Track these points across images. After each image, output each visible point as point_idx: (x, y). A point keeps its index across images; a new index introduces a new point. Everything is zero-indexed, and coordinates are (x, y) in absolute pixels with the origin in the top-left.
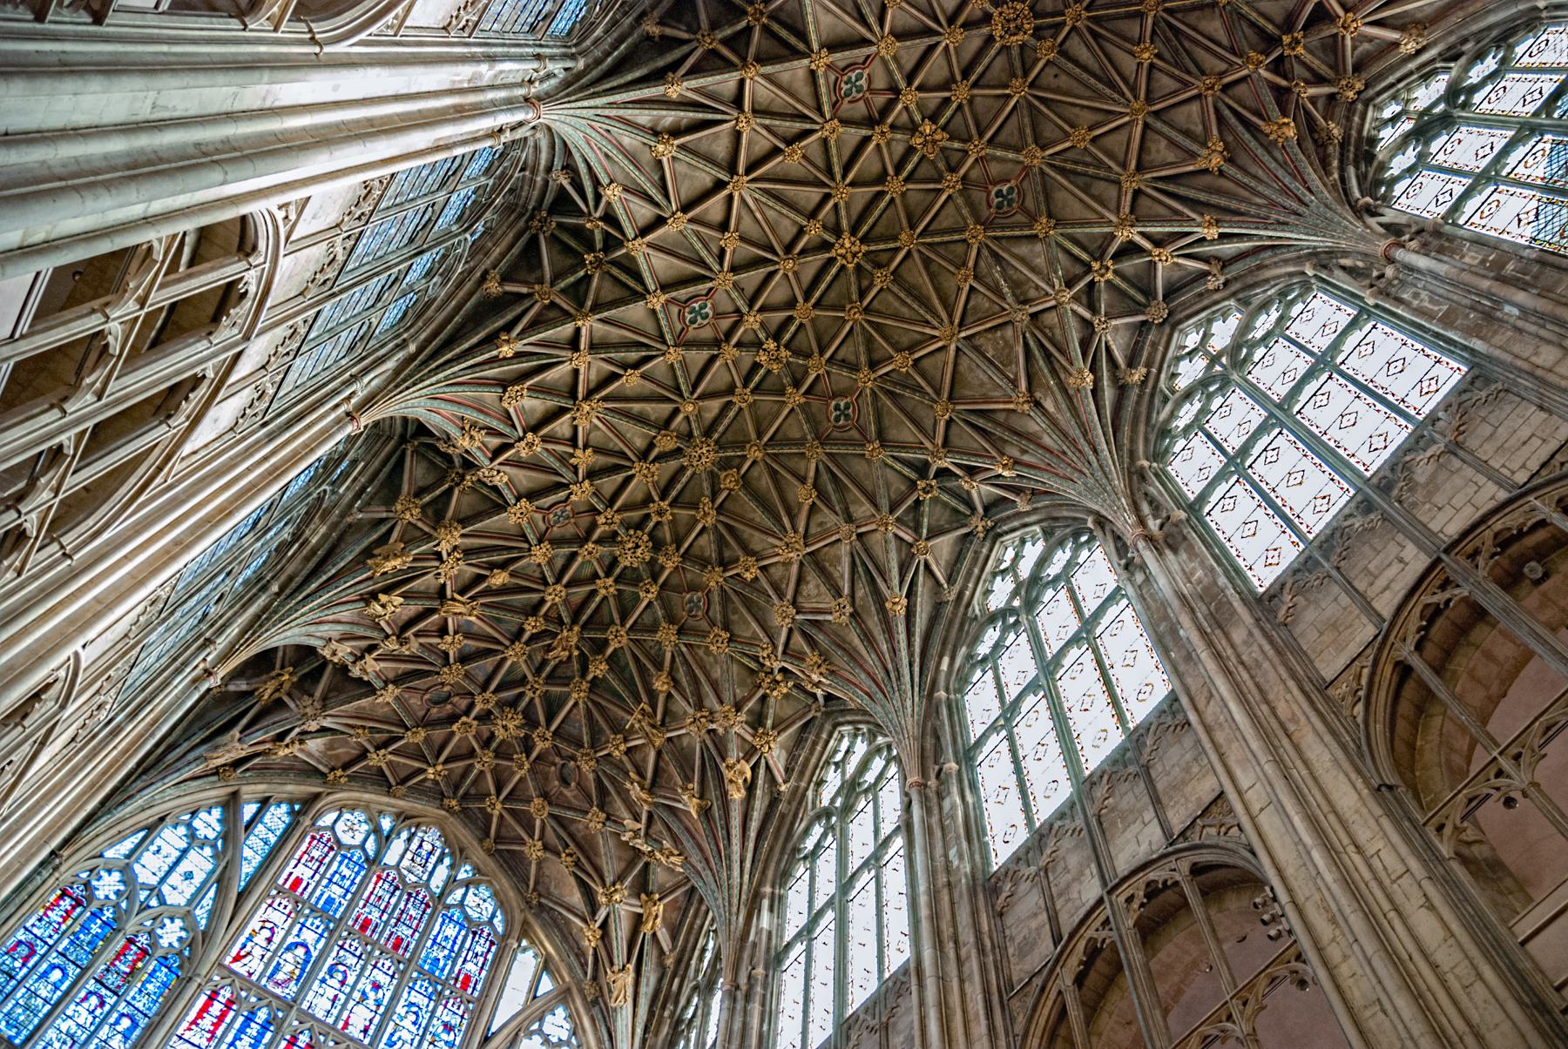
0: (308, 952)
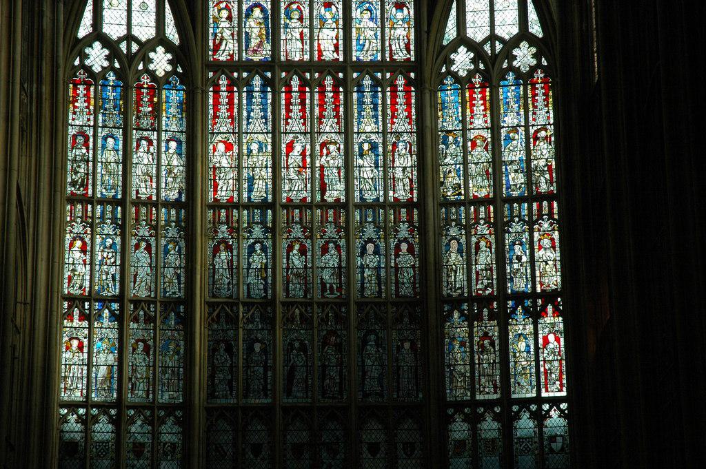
0: (263, 10)
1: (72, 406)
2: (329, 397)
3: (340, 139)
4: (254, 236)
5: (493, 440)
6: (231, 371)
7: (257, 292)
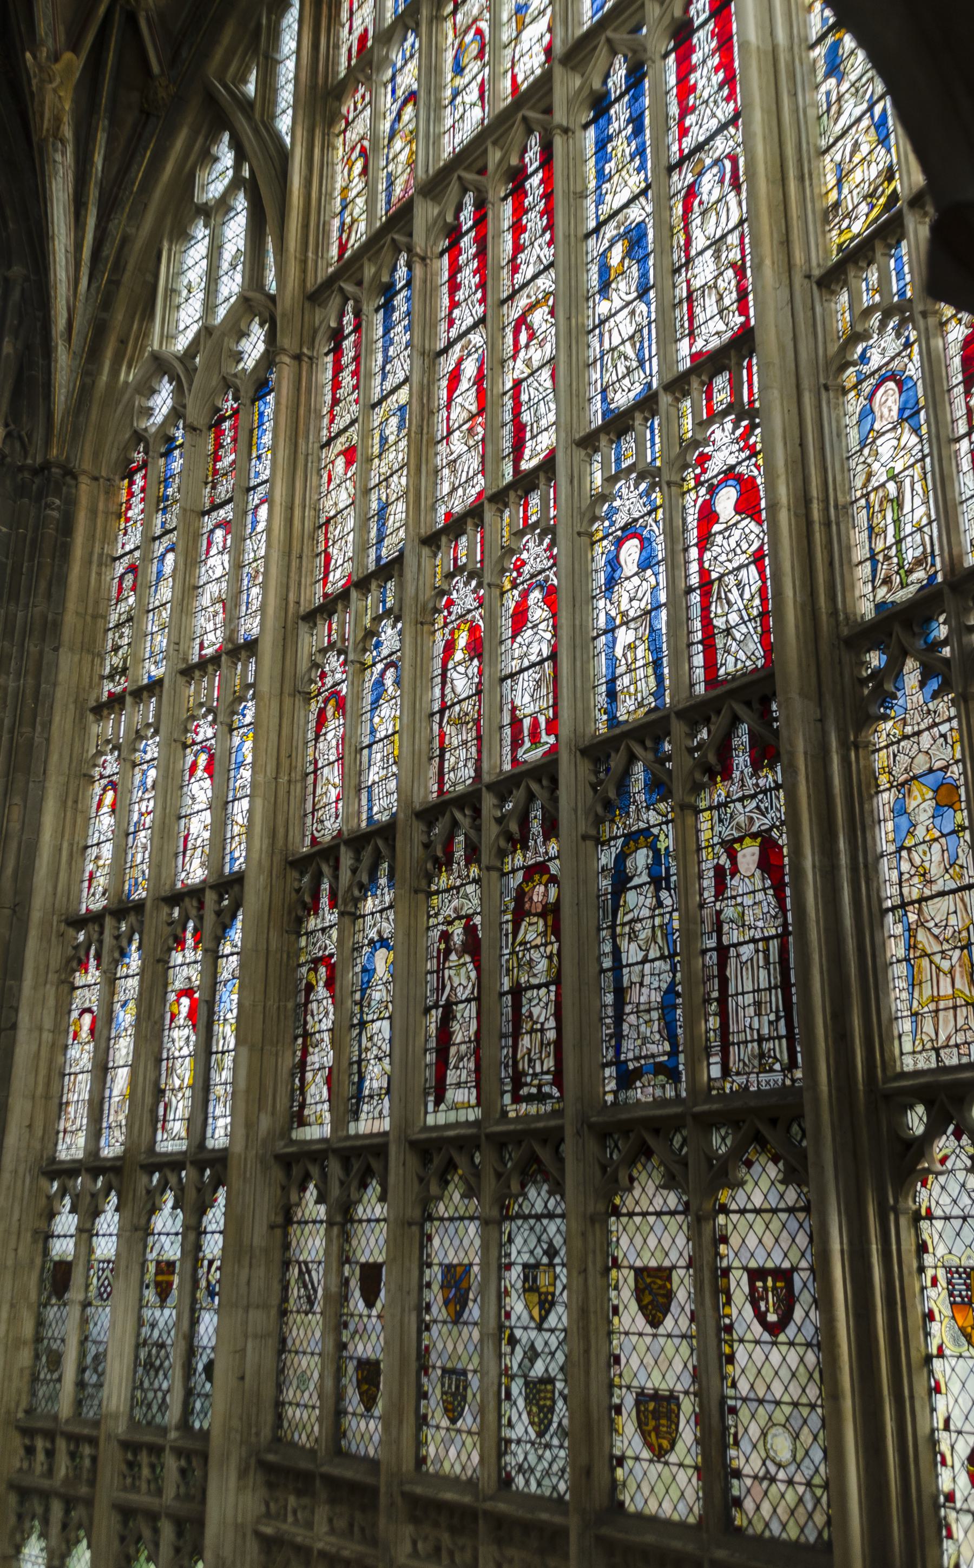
2: (529, 1099)
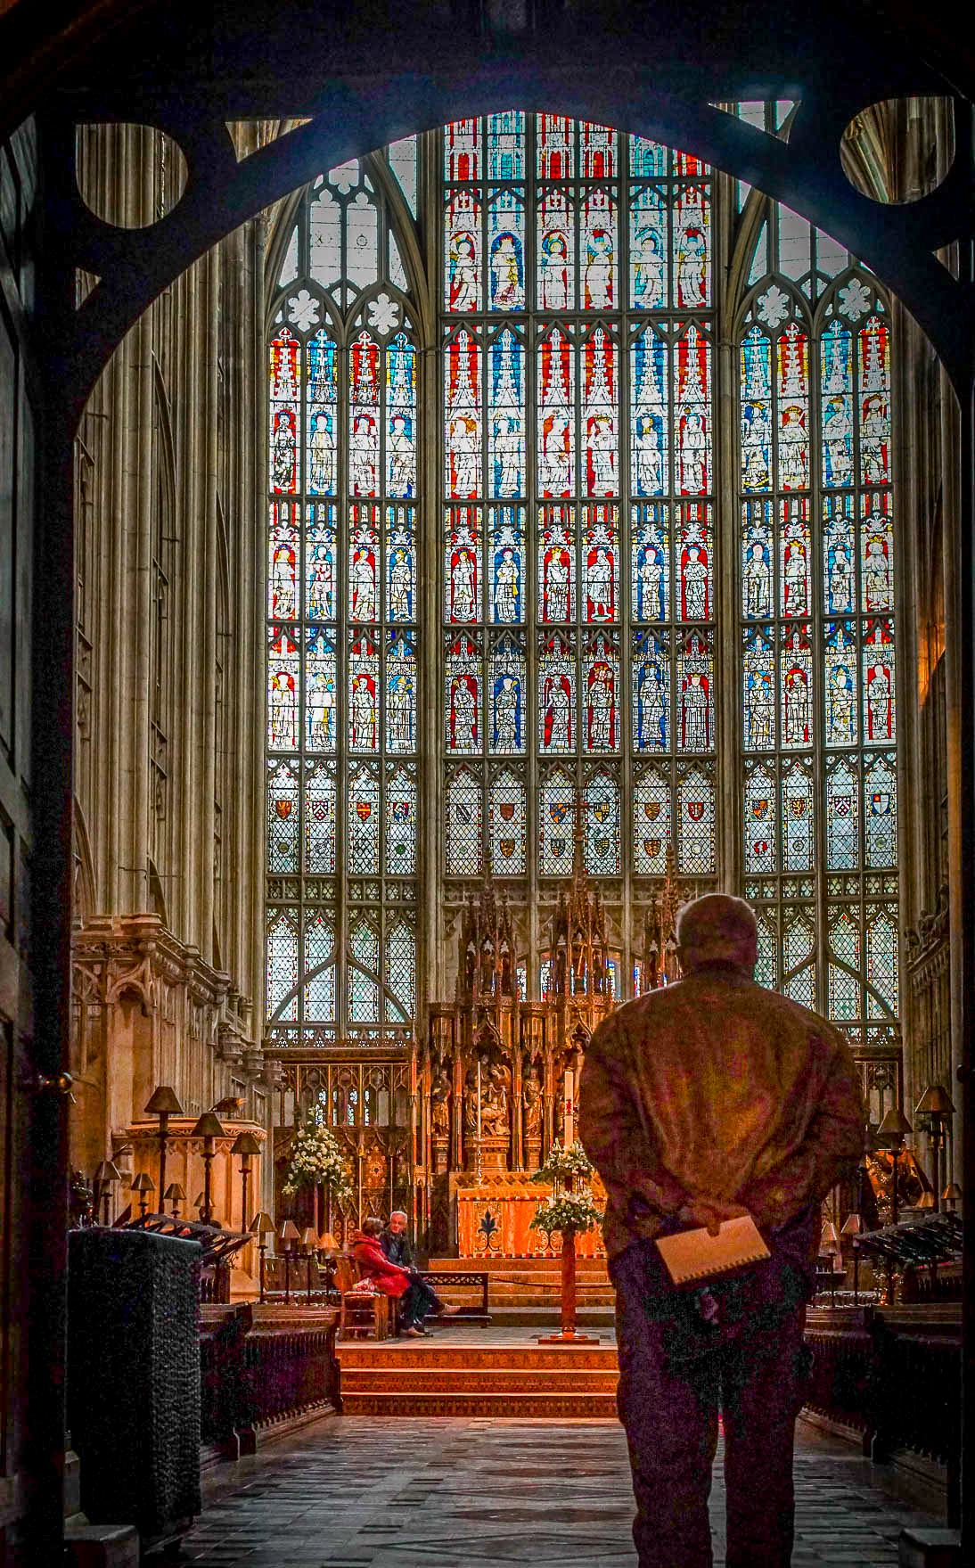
0: (514, 242)
1: (283, 757)
2: (597, 747)
3: (613, 413)
4: (503, 542)
5: (802, 801)
6: (476, 715)
7: (506, 614)
